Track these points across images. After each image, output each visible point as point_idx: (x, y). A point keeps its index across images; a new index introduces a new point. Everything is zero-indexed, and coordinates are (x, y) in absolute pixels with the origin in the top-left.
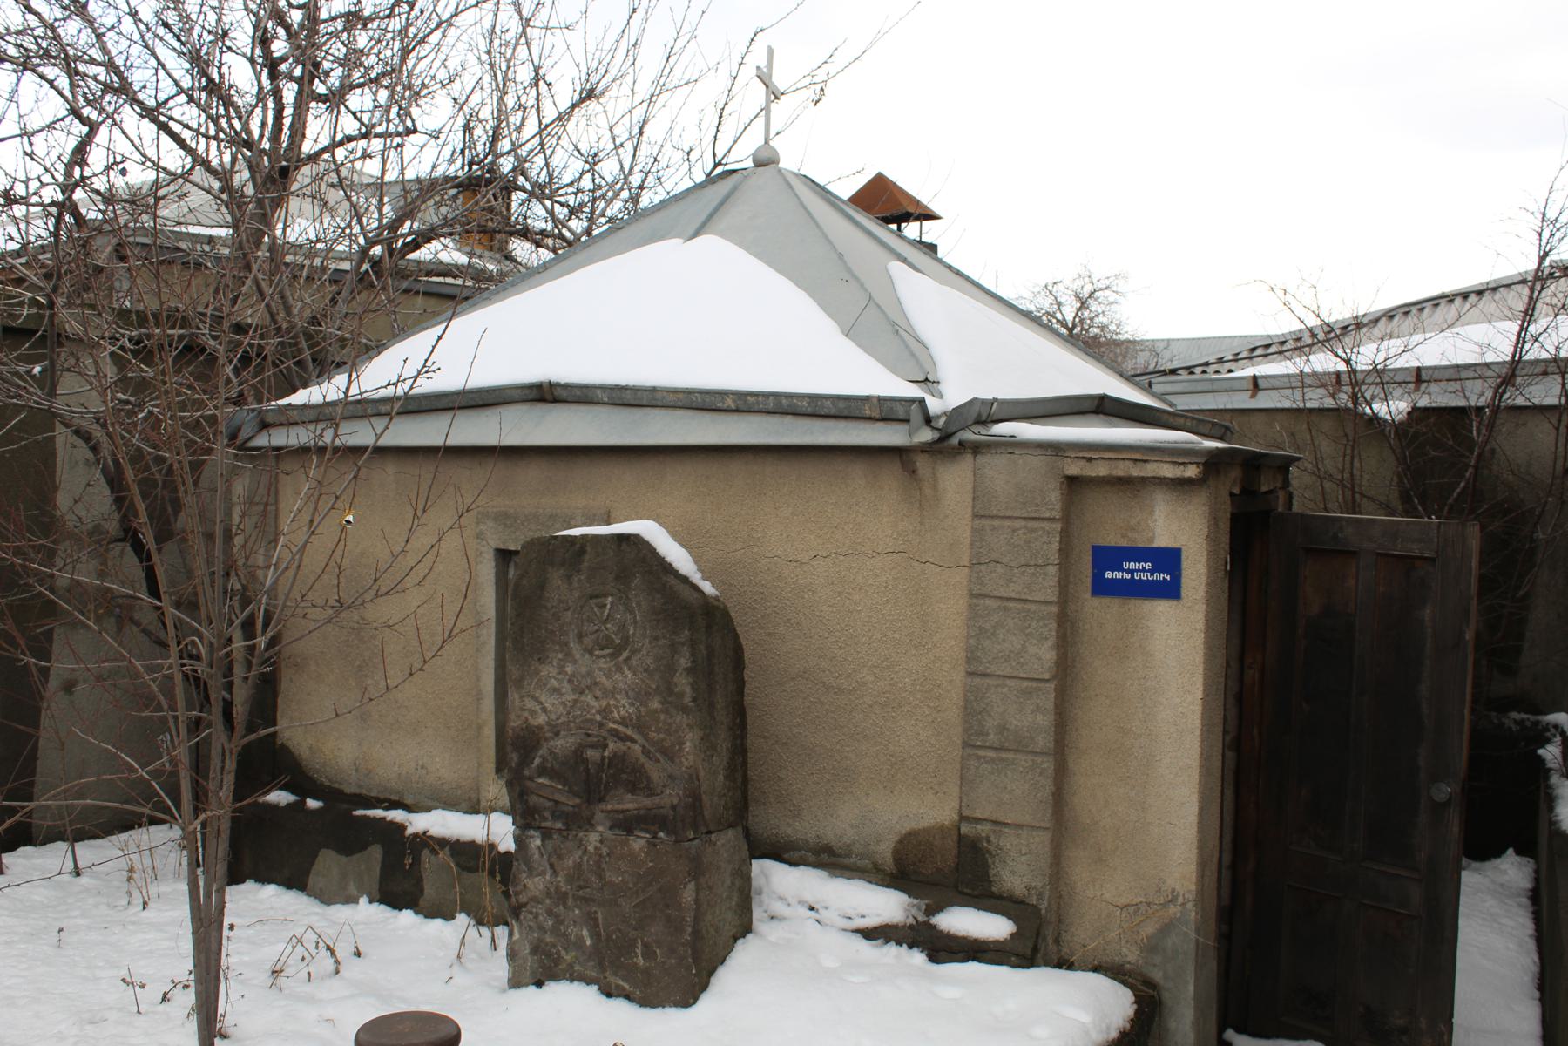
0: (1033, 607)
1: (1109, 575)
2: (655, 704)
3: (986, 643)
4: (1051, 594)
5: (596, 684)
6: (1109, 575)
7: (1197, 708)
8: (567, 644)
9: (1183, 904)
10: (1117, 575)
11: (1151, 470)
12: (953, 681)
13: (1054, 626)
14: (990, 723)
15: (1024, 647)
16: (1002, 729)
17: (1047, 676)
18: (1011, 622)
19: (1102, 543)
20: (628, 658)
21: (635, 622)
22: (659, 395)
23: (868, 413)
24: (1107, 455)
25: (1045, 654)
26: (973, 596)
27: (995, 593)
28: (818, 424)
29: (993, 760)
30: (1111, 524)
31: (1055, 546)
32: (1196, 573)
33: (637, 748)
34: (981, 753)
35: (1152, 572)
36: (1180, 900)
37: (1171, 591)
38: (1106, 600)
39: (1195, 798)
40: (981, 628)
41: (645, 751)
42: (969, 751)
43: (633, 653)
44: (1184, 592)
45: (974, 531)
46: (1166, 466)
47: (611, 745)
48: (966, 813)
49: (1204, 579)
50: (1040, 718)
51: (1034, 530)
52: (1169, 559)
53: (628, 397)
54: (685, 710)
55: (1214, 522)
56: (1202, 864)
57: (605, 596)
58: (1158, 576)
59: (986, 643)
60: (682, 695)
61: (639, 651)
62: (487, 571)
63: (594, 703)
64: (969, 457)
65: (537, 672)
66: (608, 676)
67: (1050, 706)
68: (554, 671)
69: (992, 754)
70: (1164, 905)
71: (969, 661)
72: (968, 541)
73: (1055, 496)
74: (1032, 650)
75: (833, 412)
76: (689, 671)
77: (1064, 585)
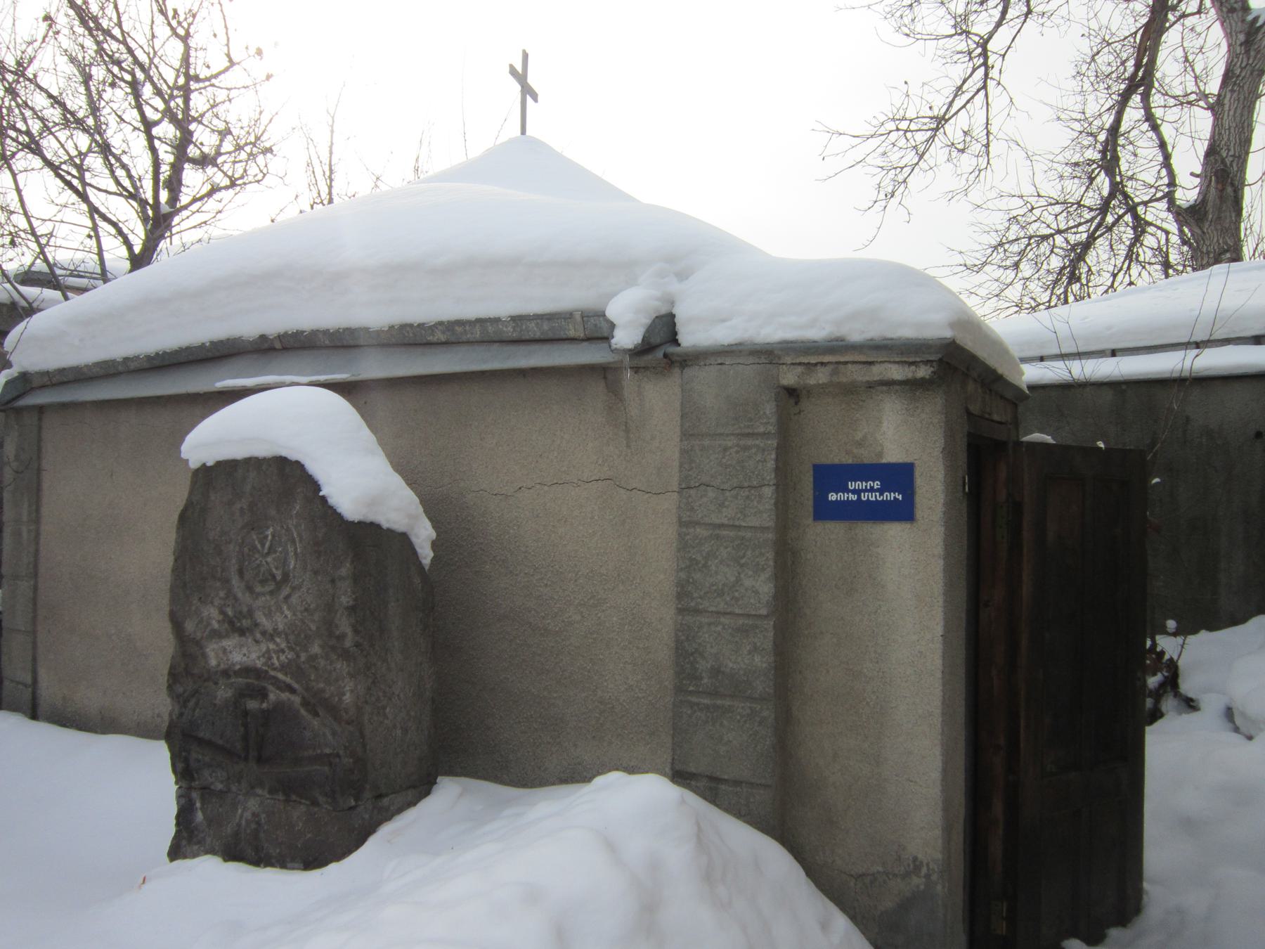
0: (749, 535)
1: (833, 497)
2: (316, 649)
3: (698, 576)
4: (767, 520)
5: (257, 625)
6: (833, 497)
7: (938, 646)
8: (227, 581)
9: (928, 876)
10: (842, 496)
11: (878, 372)
12: (663, 617)
13: (771, 555)
14: (703, 665)
15: (738, 580)
16: (716, 672)
17: (764, 612)
19: (824, 461)
20: (287, 598)
21: (296, 553)
23: (572, 333)
24: (826, 359)
25: (762, 586)
27: (707, 520)
28: (523, 349)
29: (707, 707)
30: (830, 437)
31: (771, 464)
32: (933, 491)
33: (296, 700)
34: (694, 699)
35: (881, 491)
36: (924, 870)
37: (903, 512)
38: (830, 525)
39: (937, 751)
40: (691, 559)
41: (305, 703)
43: (293, 589)
44: (919, 513)
45: (683, 452)
46: (894, 367)
47: (272, 697)
49: (941, 498)
50: (757, 659)
51: (746, 448)
52: (899, 476)
54: (345, 655)
55: (950, 435)
56: (948, 829)
58: (889, 496)
59: (698, 576)
60: (341, 637)
61: (299, 587)
64: (677, 371)
66: (269, 615)
67: (769, 645)
69: (706, 701)
70: (907, 875)
71: (679, 596)
72: (676, 464)
73: (769, 409)
74: (748, 583)
75: (538, 335)
76: (352, 609)
77: (783, 506)
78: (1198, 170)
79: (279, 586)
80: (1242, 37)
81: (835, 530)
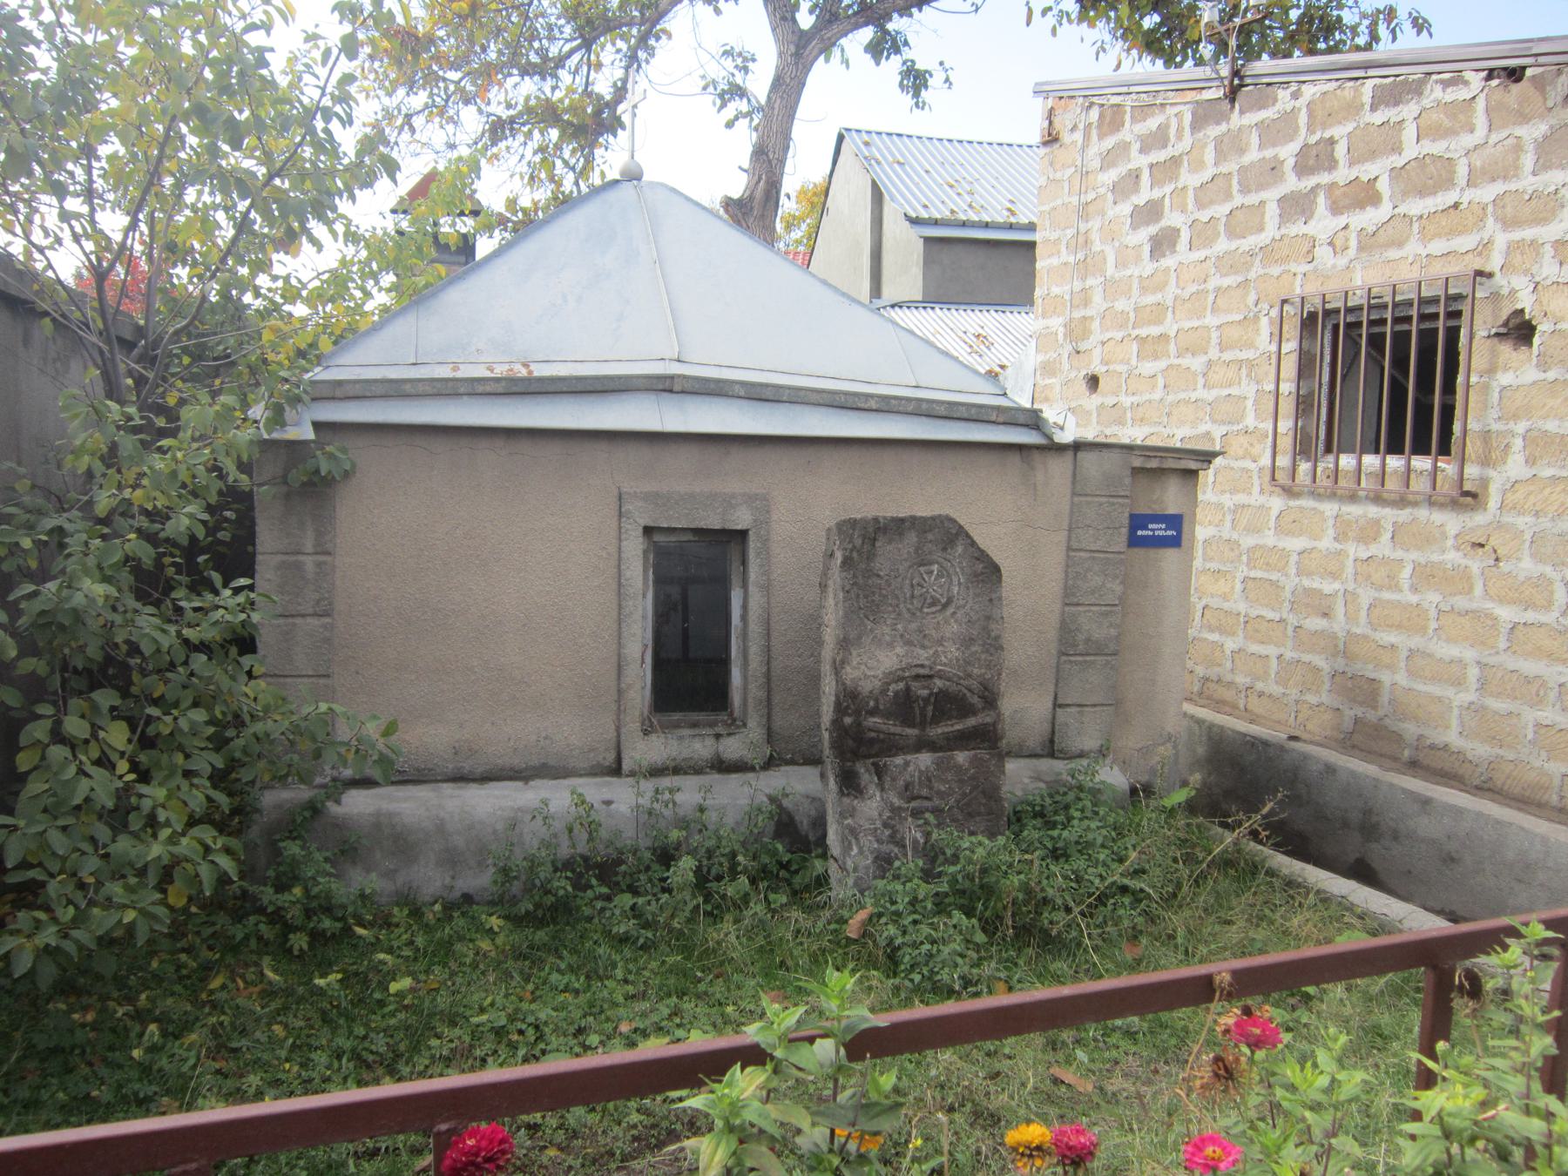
1: (1140, 533)
6: (1140, 533)
10: (1145, 533)
11: (1171, 464)
14: (1081, 637)
18: (1096, 568)
22: (802, 393)
26: (1069, 549)
38: (1136, 550)
42: (1064, 658)
43: (958, 608)
48: (1060, 701)
53: (768, 394)
57: (931, 563)
58: (1169, 533)
62: (635, 546)
63: (921, 652)
65: (872, 630)
68: (887, 630)
71: (1066, 595)
73: (1127, 481)
75: (965, 415)
78: (746, 165)
79: (945, 606)
80: (792, 48)
81: (1139, 553)
